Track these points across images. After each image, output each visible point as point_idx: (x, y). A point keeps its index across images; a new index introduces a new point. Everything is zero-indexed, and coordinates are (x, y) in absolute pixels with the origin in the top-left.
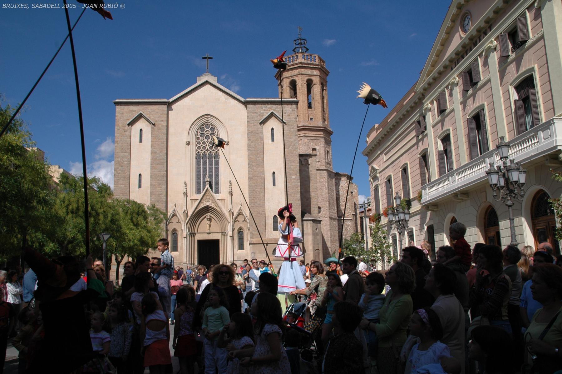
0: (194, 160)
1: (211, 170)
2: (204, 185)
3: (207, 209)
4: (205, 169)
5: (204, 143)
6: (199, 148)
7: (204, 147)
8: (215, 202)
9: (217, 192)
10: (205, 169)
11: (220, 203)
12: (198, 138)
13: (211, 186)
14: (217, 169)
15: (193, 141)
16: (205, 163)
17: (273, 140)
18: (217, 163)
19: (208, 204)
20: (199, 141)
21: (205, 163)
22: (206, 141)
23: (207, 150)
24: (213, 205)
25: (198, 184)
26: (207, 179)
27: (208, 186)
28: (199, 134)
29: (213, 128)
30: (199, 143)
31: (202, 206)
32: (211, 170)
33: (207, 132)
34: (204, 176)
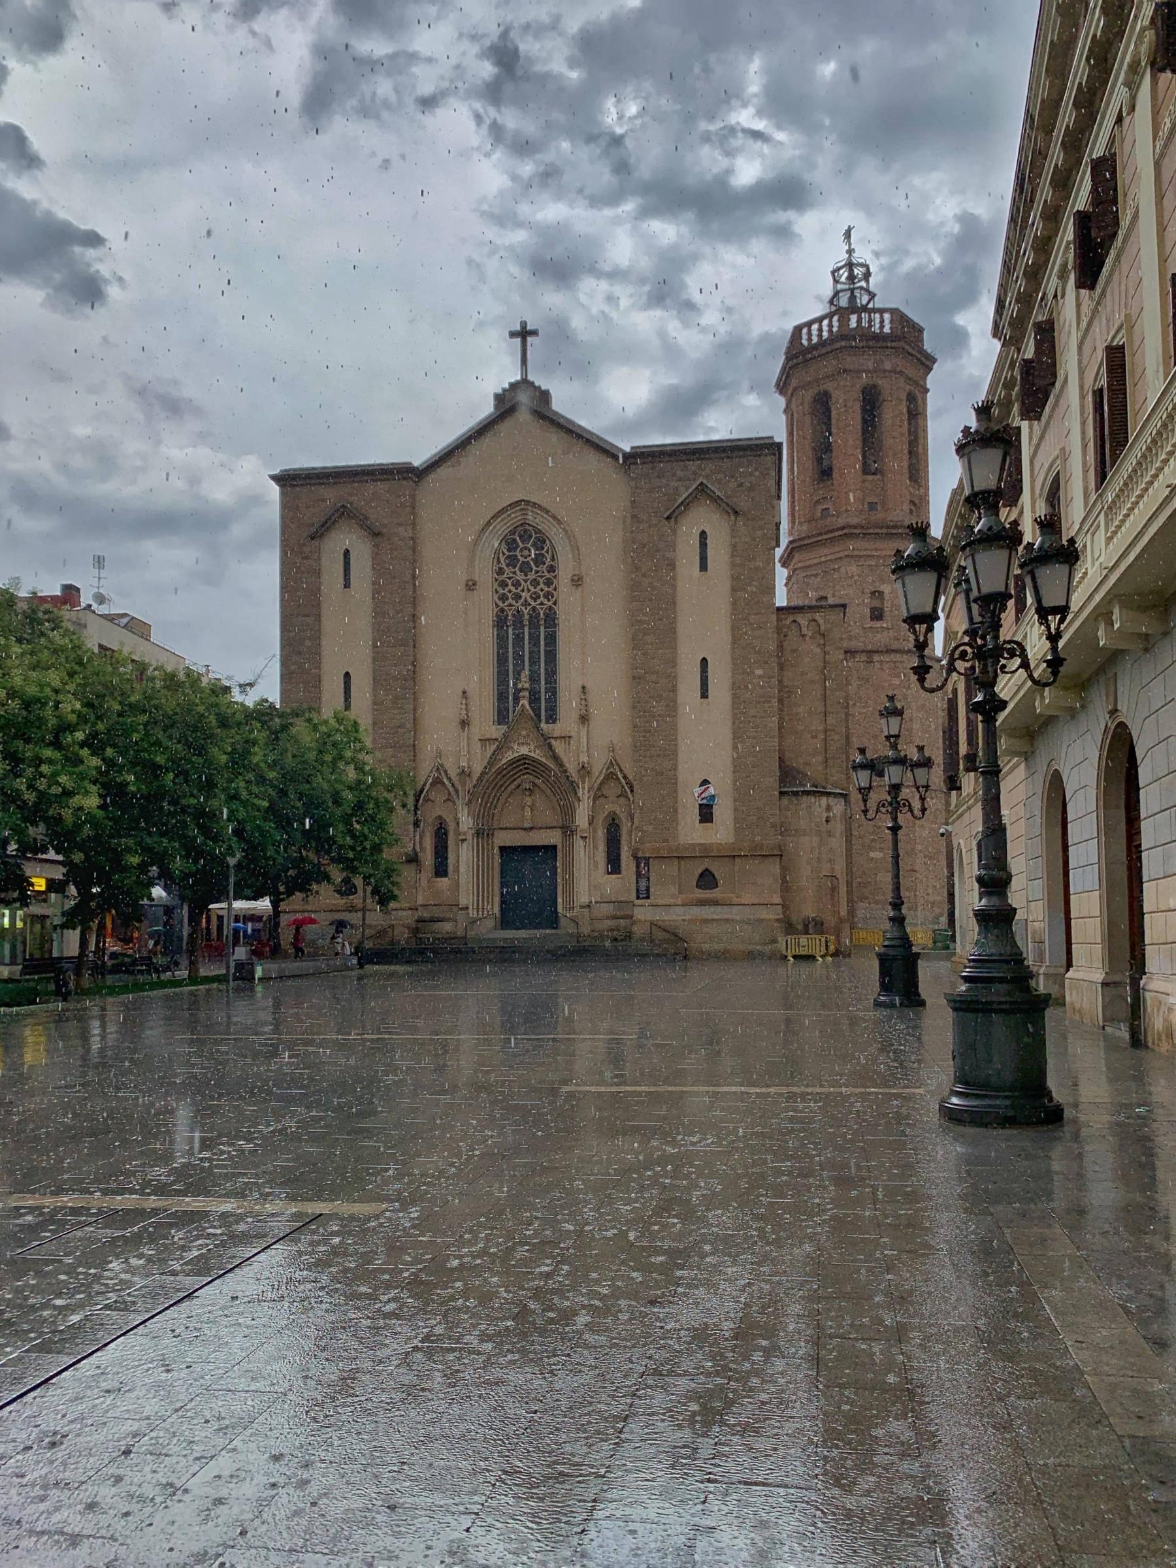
0: (489, 634)
1: (534, 661)
2: (516, 699)
3: (524, 764)
4: (519, 657)
5: (517, 584)
6: (503, 598)
7: (517, 597)
8: (546, 742)
9: (552, 718)
10: (519, 657)
11: (559, 747)
12: (500, 571)
13: (534, 699)
14: (551, 656)
15: (485, 573)
16: (519, 639)
17: (703, 567)
18: (552, 639)
19: (524, 750)
20: (501, 578)
21: (519, 639)
22: (520, 577)
23: (526, 604)
24: (537, 754)
25: (502, 697)
26: (525, 683)
27: (525, 702)
28: (502, 559)
29: (541, 541)
30: (503, 584)
31: (510, 756)
32: (534, 661)
33: (526, 553)
34: (517, 674)
